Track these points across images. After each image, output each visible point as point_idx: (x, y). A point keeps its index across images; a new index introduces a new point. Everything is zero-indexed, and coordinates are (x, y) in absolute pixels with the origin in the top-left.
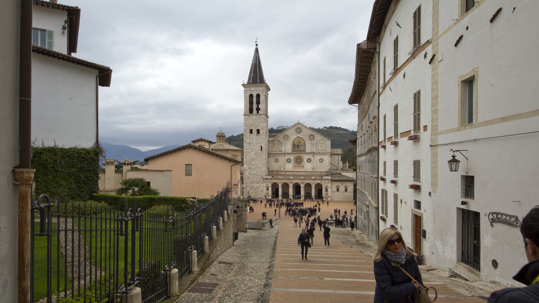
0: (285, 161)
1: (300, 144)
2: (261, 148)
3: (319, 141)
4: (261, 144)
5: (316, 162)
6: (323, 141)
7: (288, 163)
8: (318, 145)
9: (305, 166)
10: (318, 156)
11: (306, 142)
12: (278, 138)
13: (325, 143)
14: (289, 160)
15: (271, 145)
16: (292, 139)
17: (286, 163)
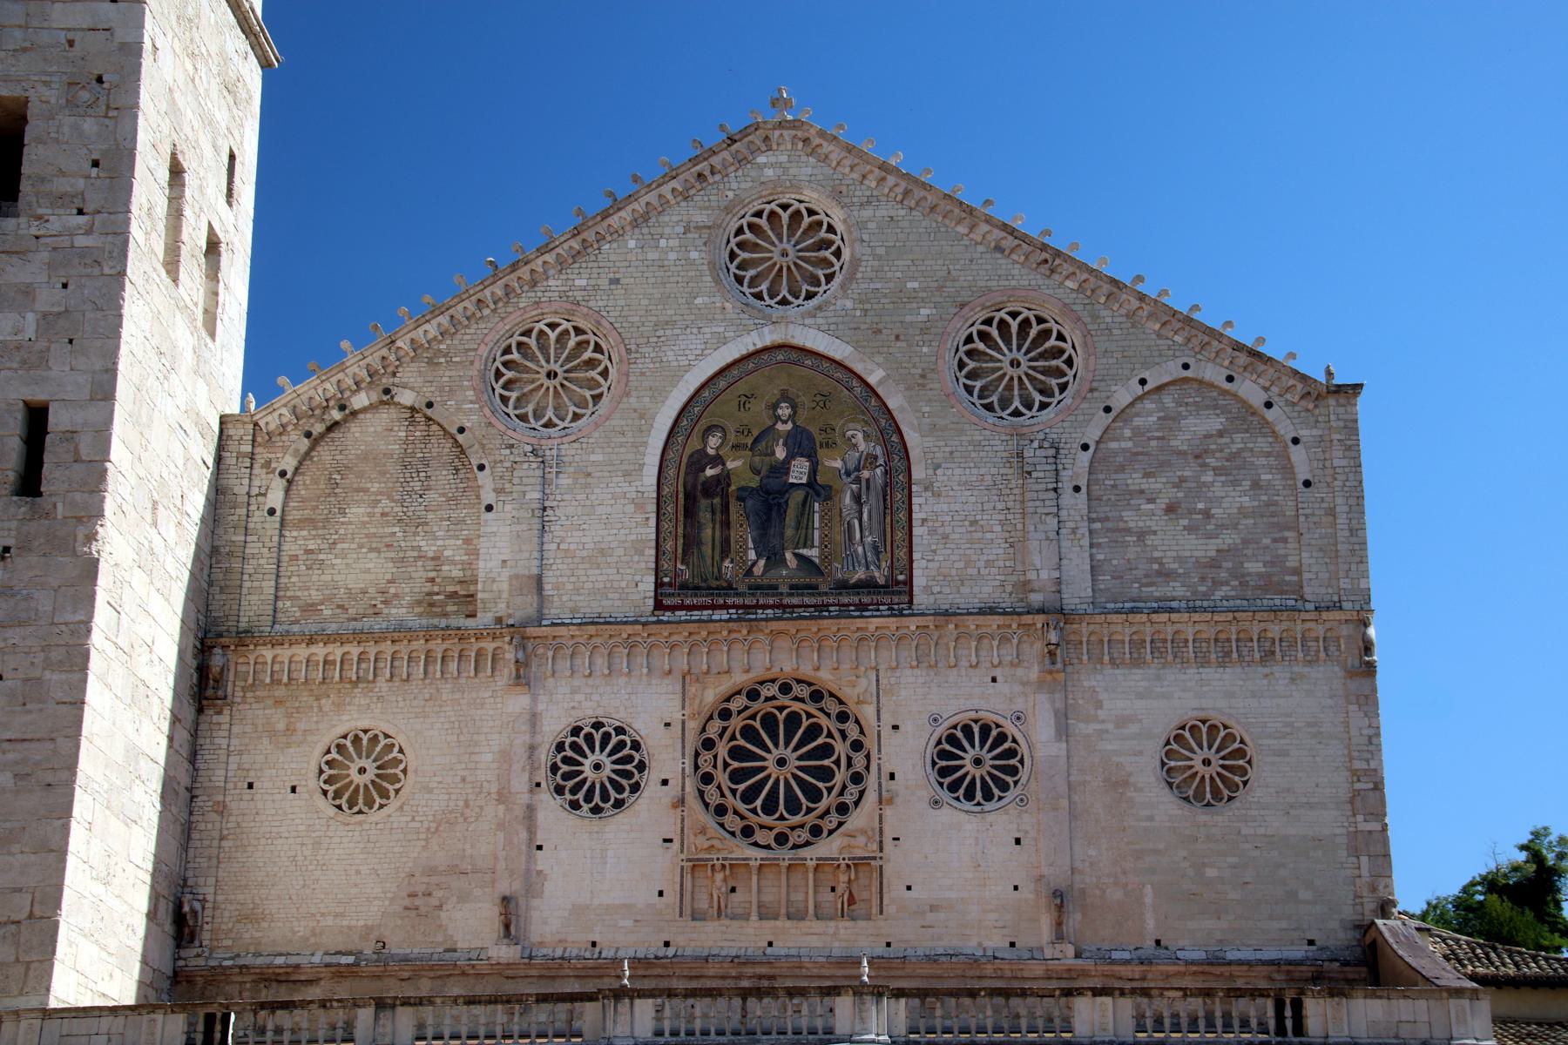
0: (520, 783)
1: (799, 472)
2: (14, 446)
3: (1148, 417)
4: (43, 358)
5: (1119, 784)
6: (1215, 423)
7: (570, 820)
8: (1135, 480)
9: (897, 863)
10: (1136, 678)
11: (911, 437)
12: (408, 374)
13: (1263, 443)
14: (596, 766)
15: (275, 498)
16: (659, 395)
17: (551, 808)
